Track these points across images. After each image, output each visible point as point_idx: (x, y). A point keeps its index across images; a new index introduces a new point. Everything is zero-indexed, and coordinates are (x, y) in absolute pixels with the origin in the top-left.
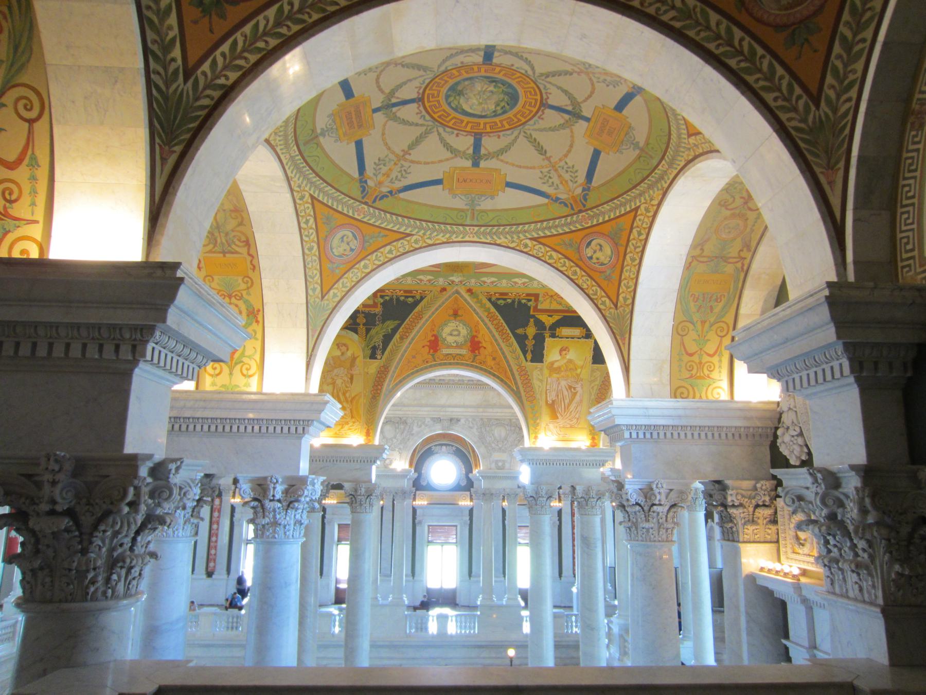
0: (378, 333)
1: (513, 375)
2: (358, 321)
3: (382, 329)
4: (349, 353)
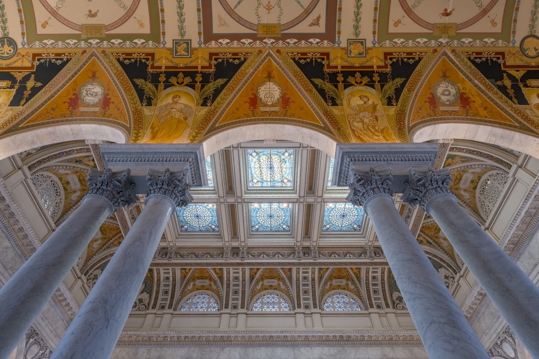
0: (391, 86)
1: (509, 115)
2: (374, 79)
3: (393, 85)
4: (370, 102)
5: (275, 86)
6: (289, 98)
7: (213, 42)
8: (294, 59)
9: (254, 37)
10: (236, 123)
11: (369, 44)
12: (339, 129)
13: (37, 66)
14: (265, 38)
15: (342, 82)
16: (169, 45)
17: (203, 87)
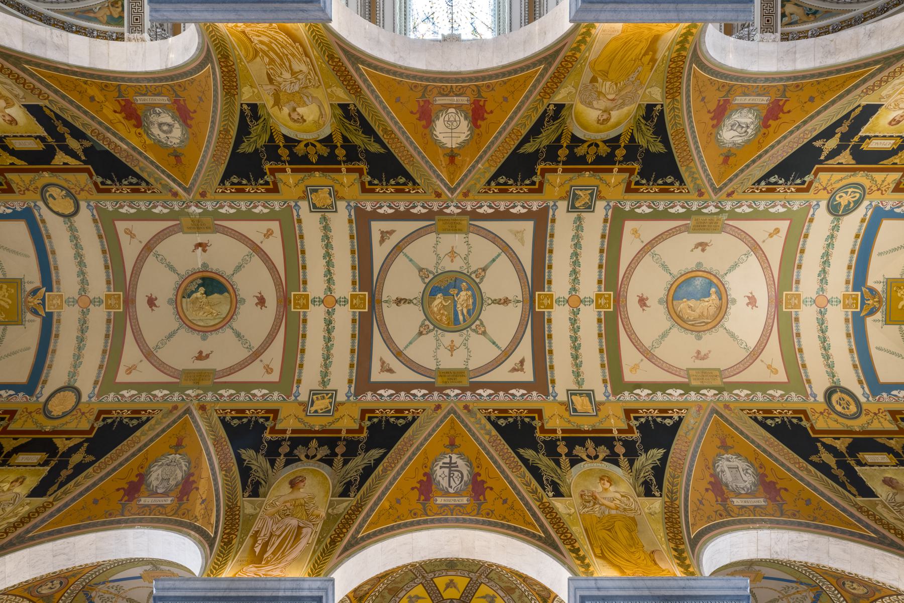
1: (48, 86)
3: (255, 142)
4: (286, 110)
5: (444, 140)
6: (420, 119)
7: (535, 209)
8: (415, 183)
9: (475, 215)
10: (510, 73)
11: (304, 205)
12: (331, 57)
13: (809, 173)
14: (458, 214)
15: (337, 147)
16: (600, 205)
17: (559, 139)
